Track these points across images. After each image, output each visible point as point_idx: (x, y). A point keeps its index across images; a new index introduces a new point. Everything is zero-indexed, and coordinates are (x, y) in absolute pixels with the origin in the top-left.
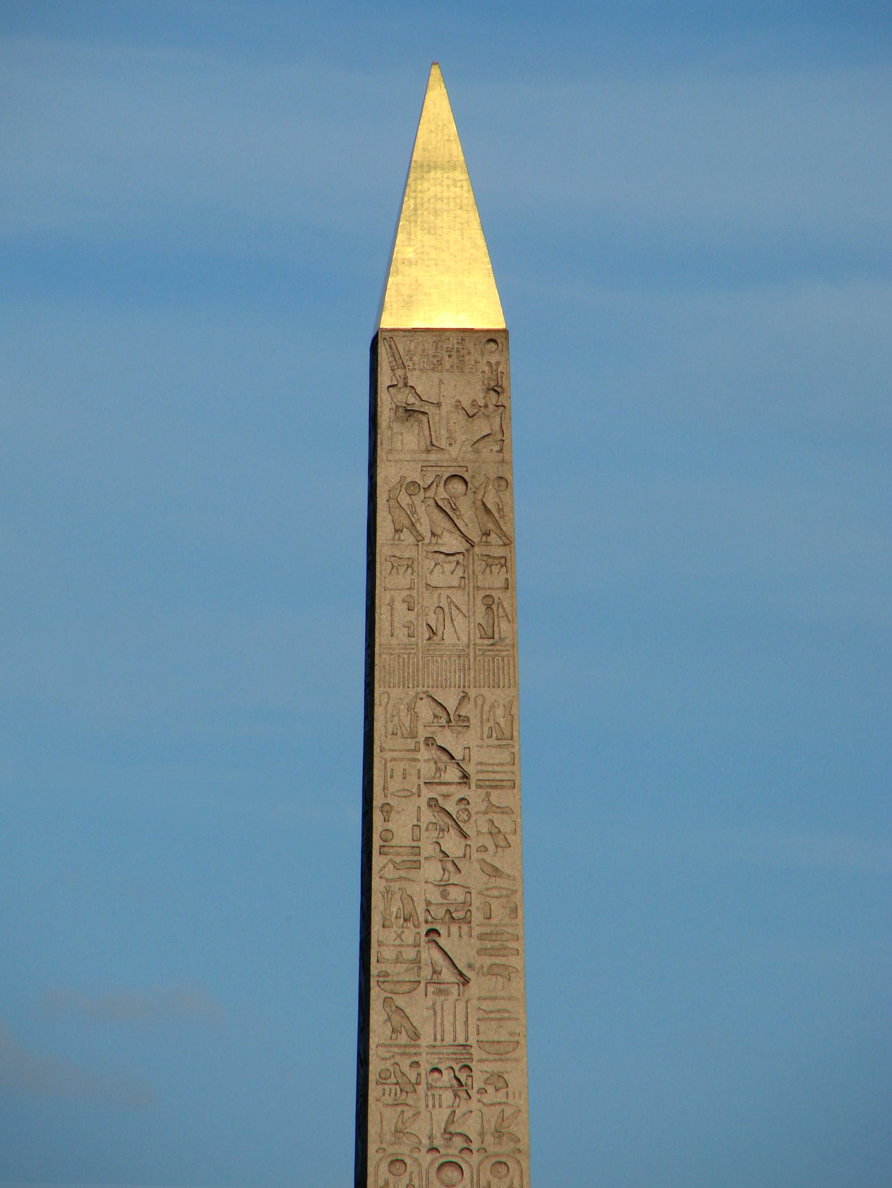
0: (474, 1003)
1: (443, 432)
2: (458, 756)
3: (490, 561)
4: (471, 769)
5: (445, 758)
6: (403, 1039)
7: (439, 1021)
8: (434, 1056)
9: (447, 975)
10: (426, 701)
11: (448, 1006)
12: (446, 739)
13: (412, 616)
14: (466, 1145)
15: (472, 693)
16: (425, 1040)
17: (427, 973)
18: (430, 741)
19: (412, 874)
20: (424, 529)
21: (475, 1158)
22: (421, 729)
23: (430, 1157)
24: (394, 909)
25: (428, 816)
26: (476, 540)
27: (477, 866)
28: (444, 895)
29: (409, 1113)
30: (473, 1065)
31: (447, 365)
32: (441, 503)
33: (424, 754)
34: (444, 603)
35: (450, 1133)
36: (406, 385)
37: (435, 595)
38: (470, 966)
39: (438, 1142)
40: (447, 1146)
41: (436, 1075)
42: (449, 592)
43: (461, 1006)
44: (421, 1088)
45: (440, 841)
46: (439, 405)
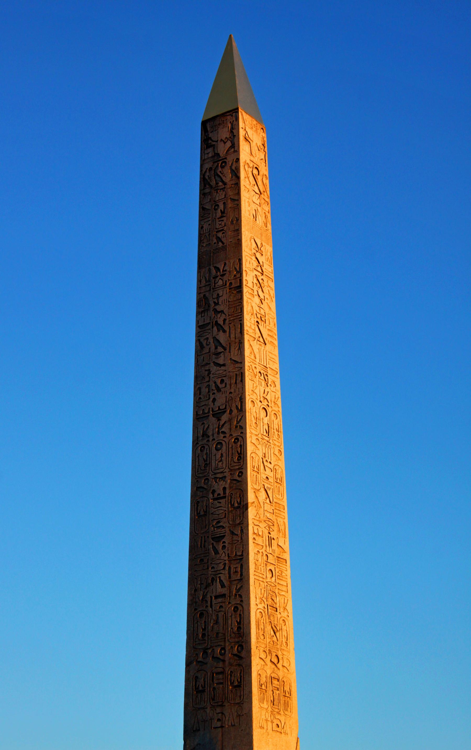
0: (267, 352)
1: (254, 151)
2: (261, 263)
6: (253, 357)
7: (260, 355)
8: (260, 367)
10: (253, 240)
12: (258, 255)
15: (263, 244)
16: (257, 360)
17: (257, 337)
19: (252, 298)
23: (260, 403)
24: (249, 309)
25: (255, 281)
27: (266, 304)
29: (255, 385)
30: (268, 375)
33: (254, 258)
39: (262, 399)
40: (264, 402)
41: (260, 375)
43: (265, 352)
44: (257, 377)
45: (258, 291)
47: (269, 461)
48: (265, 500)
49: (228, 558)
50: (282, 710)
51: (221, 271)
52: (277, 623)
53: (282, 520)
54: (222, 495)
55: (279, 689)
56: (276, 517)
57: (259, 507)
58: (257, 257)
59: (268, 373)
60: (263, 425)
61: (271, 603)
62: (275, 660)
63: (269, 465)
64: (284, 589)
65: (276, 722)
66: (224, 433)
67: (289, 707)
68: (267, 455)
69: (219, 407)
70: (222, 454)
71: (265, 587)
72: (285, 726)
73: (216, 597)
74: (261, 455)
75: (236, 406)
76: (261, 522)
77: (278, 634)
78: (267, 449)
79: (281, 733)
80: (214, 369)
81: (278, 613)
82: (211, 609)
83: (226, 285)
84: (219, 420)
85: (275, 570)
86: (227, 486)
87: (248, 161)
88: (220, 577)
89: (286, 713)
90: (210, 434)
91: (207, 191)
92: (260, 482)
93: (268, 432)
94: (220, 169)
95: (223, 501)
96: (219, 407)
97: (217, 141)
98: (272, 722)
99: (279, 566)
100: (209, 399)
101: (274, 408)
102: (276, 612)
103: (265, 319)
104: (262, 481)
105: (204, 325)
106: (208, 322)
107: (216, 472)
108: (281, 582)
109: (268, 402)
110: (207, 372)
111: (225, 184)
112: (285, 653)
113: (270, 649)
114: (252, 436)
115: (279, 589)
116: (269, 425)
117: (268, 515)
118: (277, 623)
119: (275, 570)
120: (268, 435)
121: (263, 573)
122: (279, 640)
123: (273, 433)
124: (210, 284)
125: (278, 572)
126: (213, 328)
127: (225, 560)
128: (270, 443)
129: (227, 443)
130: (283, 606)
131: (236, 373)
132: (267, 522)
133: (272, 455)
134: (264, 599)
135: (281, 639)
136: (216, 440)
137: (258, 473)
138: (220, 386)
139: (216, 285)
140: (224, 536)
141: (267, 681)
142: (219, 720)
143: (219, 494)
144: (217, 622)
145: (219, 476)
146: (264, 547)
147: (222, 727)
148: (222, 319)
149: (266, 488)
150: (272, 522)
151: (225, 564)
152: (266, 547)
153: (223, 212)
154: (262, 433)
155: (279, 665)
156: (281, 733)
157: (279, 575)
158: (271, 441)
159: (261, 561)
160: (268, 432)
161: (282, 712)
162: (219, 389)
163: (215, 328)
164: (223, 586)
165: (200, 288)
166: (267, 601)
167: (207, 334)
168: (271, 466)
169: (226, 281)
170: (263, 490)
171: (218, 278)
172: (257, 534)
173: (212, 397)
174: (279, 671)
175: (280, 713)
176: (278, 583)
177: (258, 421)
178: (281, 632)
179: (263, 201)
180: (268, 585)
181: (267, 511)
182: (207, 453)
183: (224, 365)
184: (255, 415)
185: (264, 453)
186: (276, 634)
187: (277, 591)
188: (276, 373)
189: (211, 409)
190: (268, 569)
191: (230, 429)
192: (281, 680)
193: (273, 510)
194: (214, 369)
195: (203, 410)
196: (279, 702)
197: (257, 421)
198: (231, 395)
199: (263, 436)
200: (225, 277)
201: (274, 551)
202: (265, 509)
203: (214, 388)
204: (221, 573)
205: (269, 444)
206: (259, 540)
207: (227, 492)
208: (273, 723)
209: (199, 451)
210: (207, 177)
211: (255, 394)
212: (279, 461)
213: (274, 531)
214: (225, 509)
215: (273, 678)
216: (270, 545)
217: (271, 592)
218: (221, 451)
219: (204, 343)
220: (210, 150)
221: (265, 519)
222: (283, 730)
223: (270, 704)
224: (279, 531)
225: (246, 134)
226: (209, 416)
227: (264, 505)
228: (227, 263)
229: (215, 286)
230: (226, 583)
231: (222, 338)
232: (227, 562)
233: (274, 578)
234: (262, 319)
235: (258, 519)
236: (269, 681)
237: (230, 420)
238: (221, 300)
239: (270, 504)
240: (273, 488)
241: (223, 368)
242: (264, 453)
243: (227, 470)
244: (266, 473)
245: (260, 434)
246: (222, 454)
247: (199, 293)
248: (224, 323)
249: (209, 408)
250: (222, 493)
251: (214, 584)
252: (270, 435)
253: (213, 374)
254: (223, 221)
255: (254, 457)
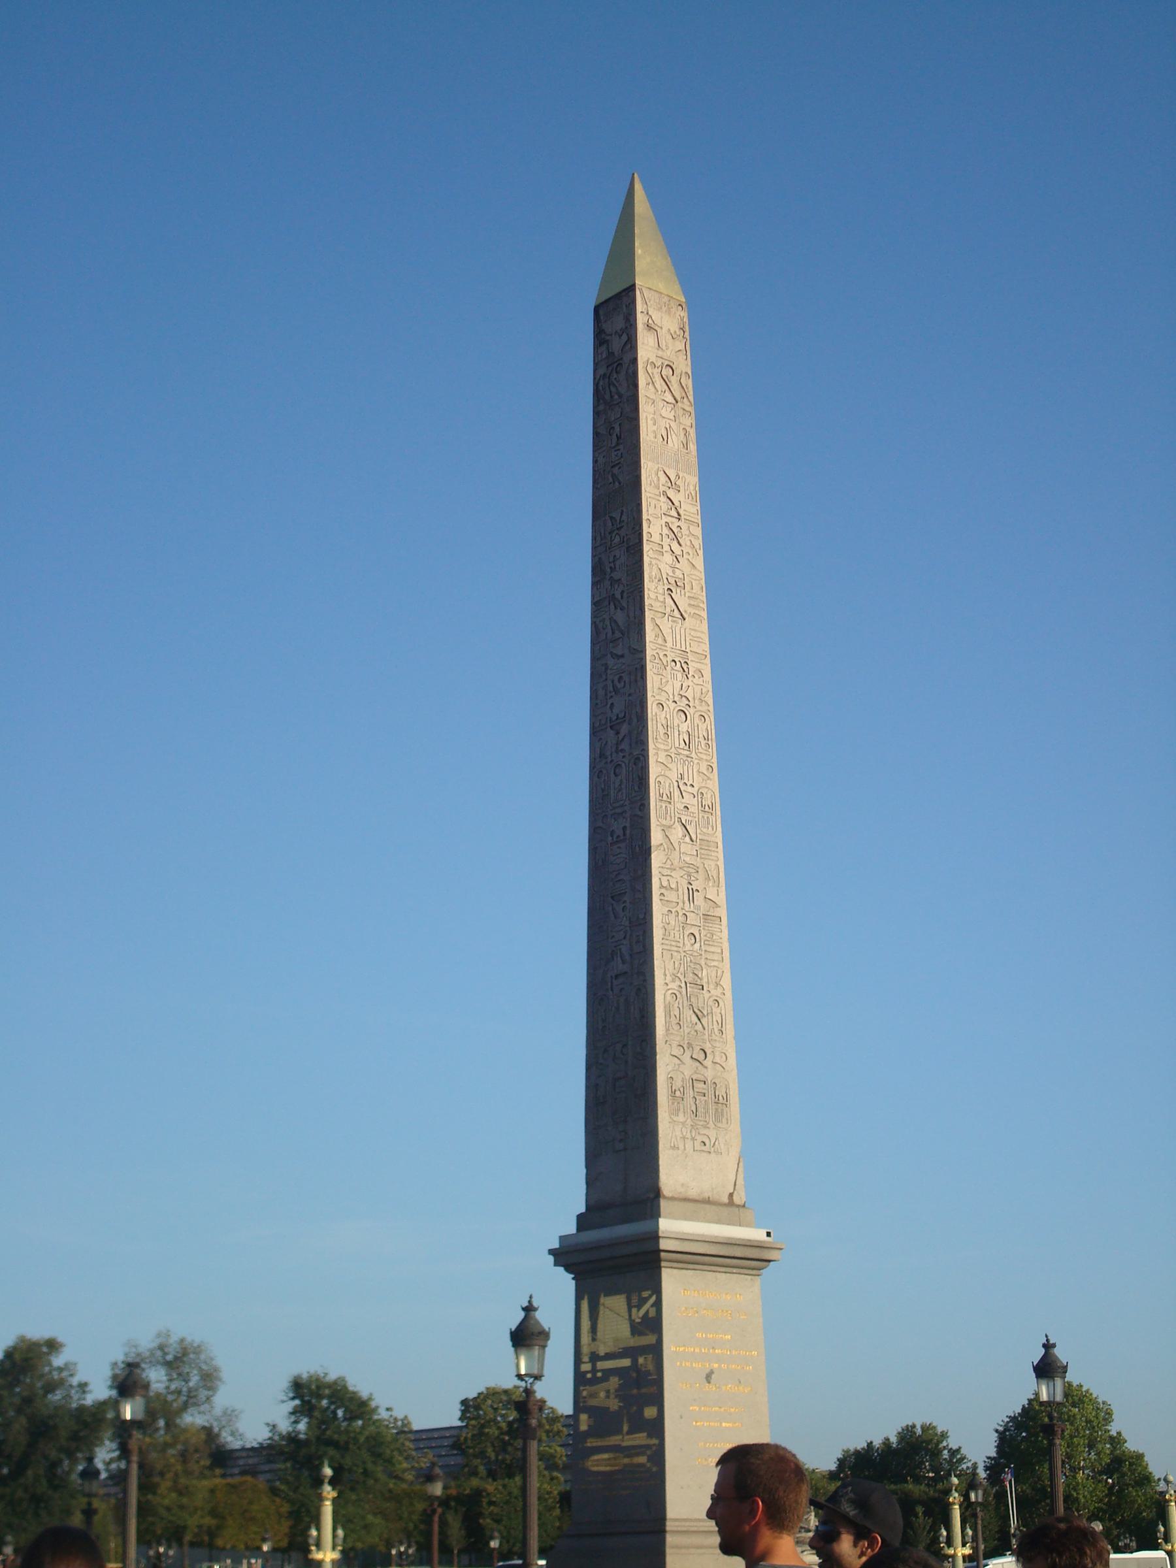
2: (677, 504)
3: (685, 412)
4: (681, 512)
5: (670, 503)
6: (660, 641)
9: (676, 613)
10: (662, 472)
11: (678, 629)
12: (671, 493)
13: (655, 428)
14: (687, 703)
16: (669, 644)
17: (668, 610)
18: (665, 493)
19: (660, 557)
20: (658, 386)
21: (692, 710)
22: (661, 486)
23: (674, 704)
24: (654, 574)
25: (666, 531)
26: (679, 399)
27: (686, 561)
28: (674, 572)
29: (664, 681)
31: (664, 309)
32: (664, 376)
33: (663, 499)
34: (668, 427)
35: (681, 695)
36: (648, 313)
37: (664, 421)
38: (685, 612)
40: (681, 702)
41: (674, 664)
42: (669, 421)
43: (683, 631)
44: (668, 668)
46: (661, 328)
47: (691, 782)
48: (681, 839)
49: (630, 923)
50: (711, 1122)
51: (618, 521)
52: (703, 1005)
53: (713, 864)
54: (622, 838)
55: (706, 1095)
56: (702, 860)
57: (671, 850)
58: (668, 495)
59: (688, 659)
60: (679, 735)
61: (691, 979)
62: (701, 1057)
63: (690, 789)
64: (716, 957)
65: (699, 1139)
66: (622, 750)
67: (725, 1116)
68: (686, 777)
69: (618, 715)
70: (621, 781)
71: (682, 958)
72: (716, 1143)
73: (617, 977)
74: (674, 776)
75: (637, 712)
76: (675, 870)
77: (704, 1021)
78: (686, 768)
79: (710, 1152)
80: (611, 662)
81: (704, 992)
82: (611, 992)
83: (623, 542)
84: (618, 733)
85: (700, 934)
86: (628, 825)
87: (653, 359)
88: (620, 949)
89: (719, 1125)
90: (608, 753)
91: (601, 408)
92: (673, 815)
93: (688, 744)
94: (615, 376)
95: (623, 845)
96: (618, 715)
97: (611, 335)
98: (693, 1139)
99: (708, 927)
100: (606, 705)
101: (698, 708)
102: (701, 991)
103: (684, 584)
104: (676, 813)
105: (600, 600)
106: (604, 596)
107: (614, 805)
108: (712, 949)
109: (689, 701)
110: (603, 668)
111: (620, 396)
112: (717, 1044)
113: (690, 1042)
114: (659, 752)
115: (707, 959)
116: (691, 733)
117: (687, 859)
118: (703, 1005)
119: (700, 934)
120: (689, 747)
121: (678, 940)
122: (706, 1028)
123: (697, 744)
124: (605, 543)
125: (706, 936)
126: (609, 604)
127: (626, 926)
128: (692, 758)
129: (627, 764)
130: (714, 981)
131: (635, 666)
132: (685, 869)
133: (695, 774)
134: (679, 975)
135: (711, 1027)
136: (615, 761)
137: (670, 803)
138: (619, 686)
139: (613, 543)
140: (626, 892)
141: (685, 1085)
142: (621, 1141)
143: (618, 836)
144: (618, 1008)
145: (619, 810)
146: (681, 904)
147: (625, 1149)
148: (620, 590)
149: (684, 822)
150: (695, 868)
151: (626, 932)
152: (684, 903)
153: (618, 438)
154: (677, 745)
155: (708, 1062)
156: (710, 1152)
157: (707, 939)
158: (693, 755)
159: (674, 923)
160: (688, 744)
161: (711, 1125)
162: (616, 690)
163: (612, 606)
164: (624, 962)
165: (595, 547)
166: (685, 977)
167: (603, 613)
168: (695, 791)
169: (624, 537)
170: (679, 826)
171: (615, 532)
172: (668, 887)
173: (610, 702)
174: (706, 1070)
175: (708, 1126)
176: (706, 951)
177: (669, 729)
178: (710, 1017)
179: (681, 412)
180: (688, 956)
181: (686, 854)
182: (605, 780)
183: (622, 656)
184: (664, 722)
185: (681, 774)
186: (701, 1020)
187: (703, 963)
188: (704, 657)
189: (609, 719)
190: (687, 933)
191: (630, 745)
192: (709, 1082)
193: (697, 850)
194: (611, 662)
195: (600, 720)
196: (707, 1112)
197: (668, 731)
198: (630, 698)
199: (678, 750)
200: (622, 530)
201: (699, 908)
202: (682, 852)
203: (611, 689)
204: (623, 944)
205: (689, 759)
206: (670, 896)
207: (628, 832)
208: (695, 1142)
209: (596, 779)
210: (601, 388)
211: (663, 693)
212: (708, 781)
213: (697, 879)
214: (624, 856)
215: (696, 1080)
216: (691, 899)
217: (692, 965)
218: (620, 777)
219: (600, 625)
220: (604, 347)
221: (681, 865)
222: (712, 1149)
223: (689, 1115)
224: (708, 878)
225: (650, 319)
226: (606, 728)
227: (680, 846)
228: (625, 510)
229: (611, 544)
230: (627, 958)
231: (620, 617)
232: (628, 928)
233: (697, 946)
234: (678, 584)
235: (669, 866)
236: (688, 1085)
237: (630, 733)
238: (618, 563)
239: (691, 842)
240: (697, 819)
241: (621, 660)
242: (681, 774)
243: (627, 803)
244: (683, 801)
245: (673, 747)
246: (621, 781)
247: (593, 556)
248: (622, 598)
249: (607, 718)
250: (620, 833)
251: (615, 958)
252: (691, 747)
253: (611, 669)
254: (619, 450)
255: (662, 783)
